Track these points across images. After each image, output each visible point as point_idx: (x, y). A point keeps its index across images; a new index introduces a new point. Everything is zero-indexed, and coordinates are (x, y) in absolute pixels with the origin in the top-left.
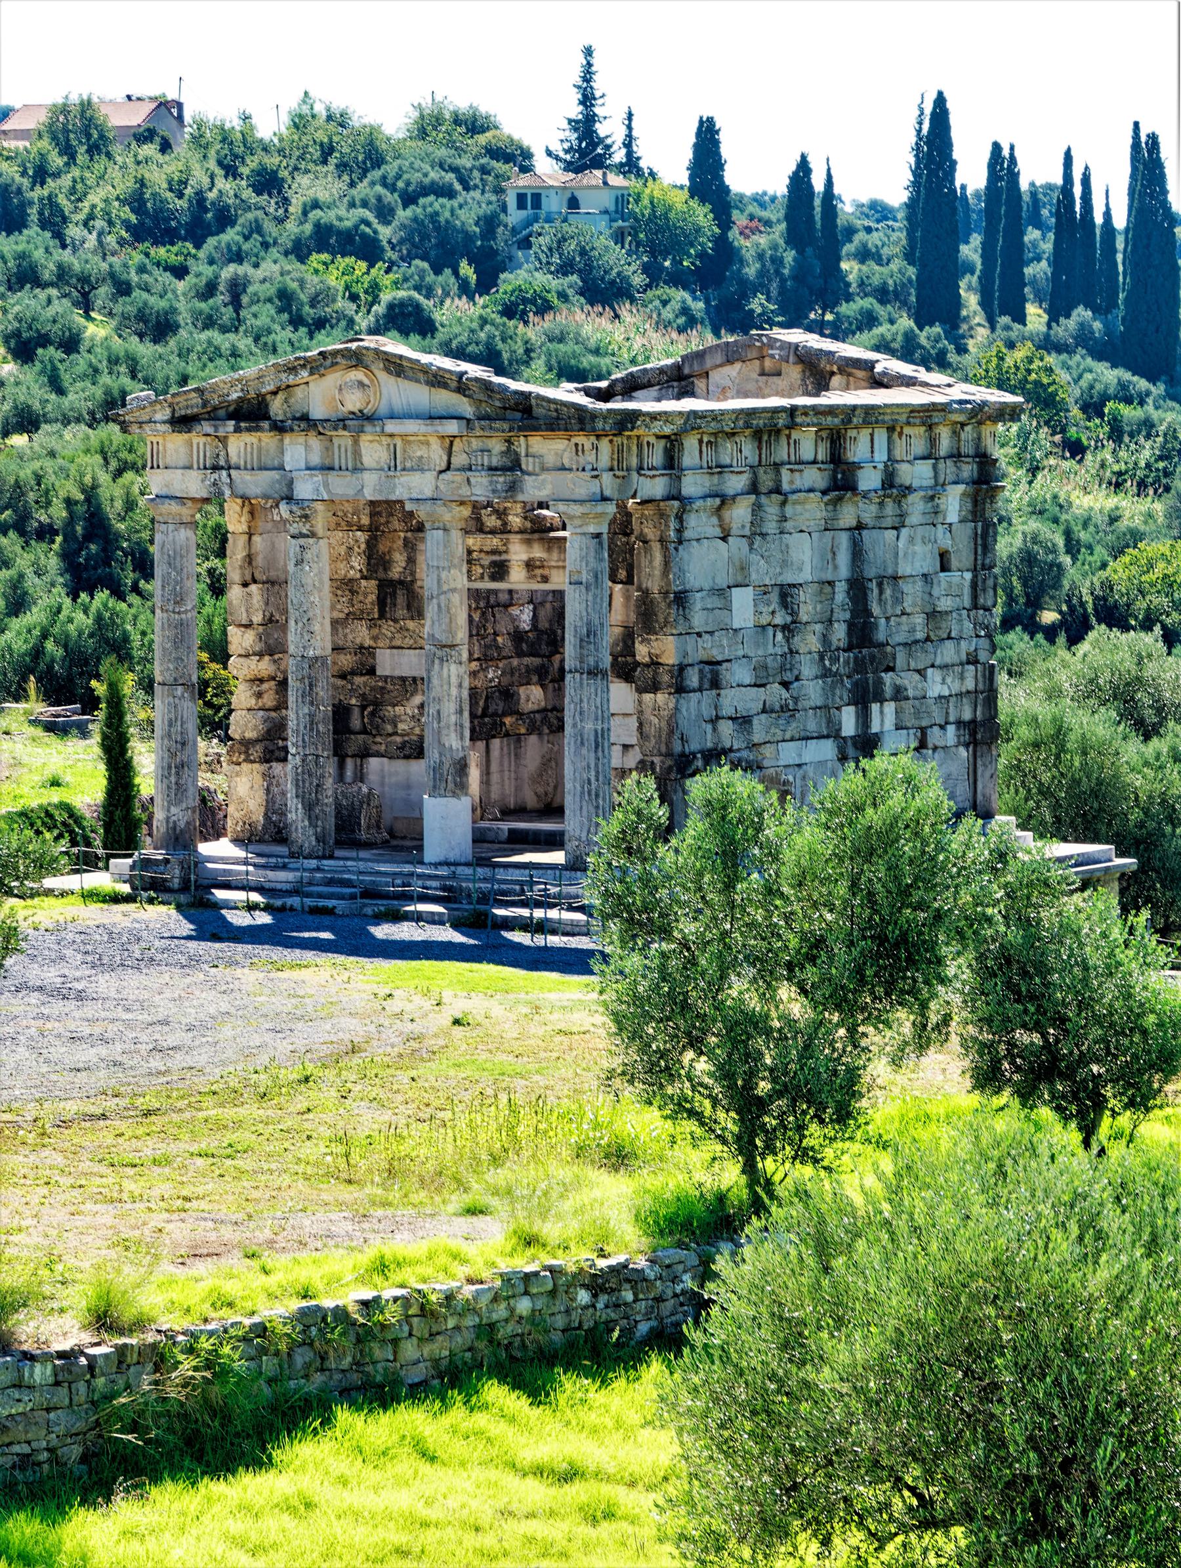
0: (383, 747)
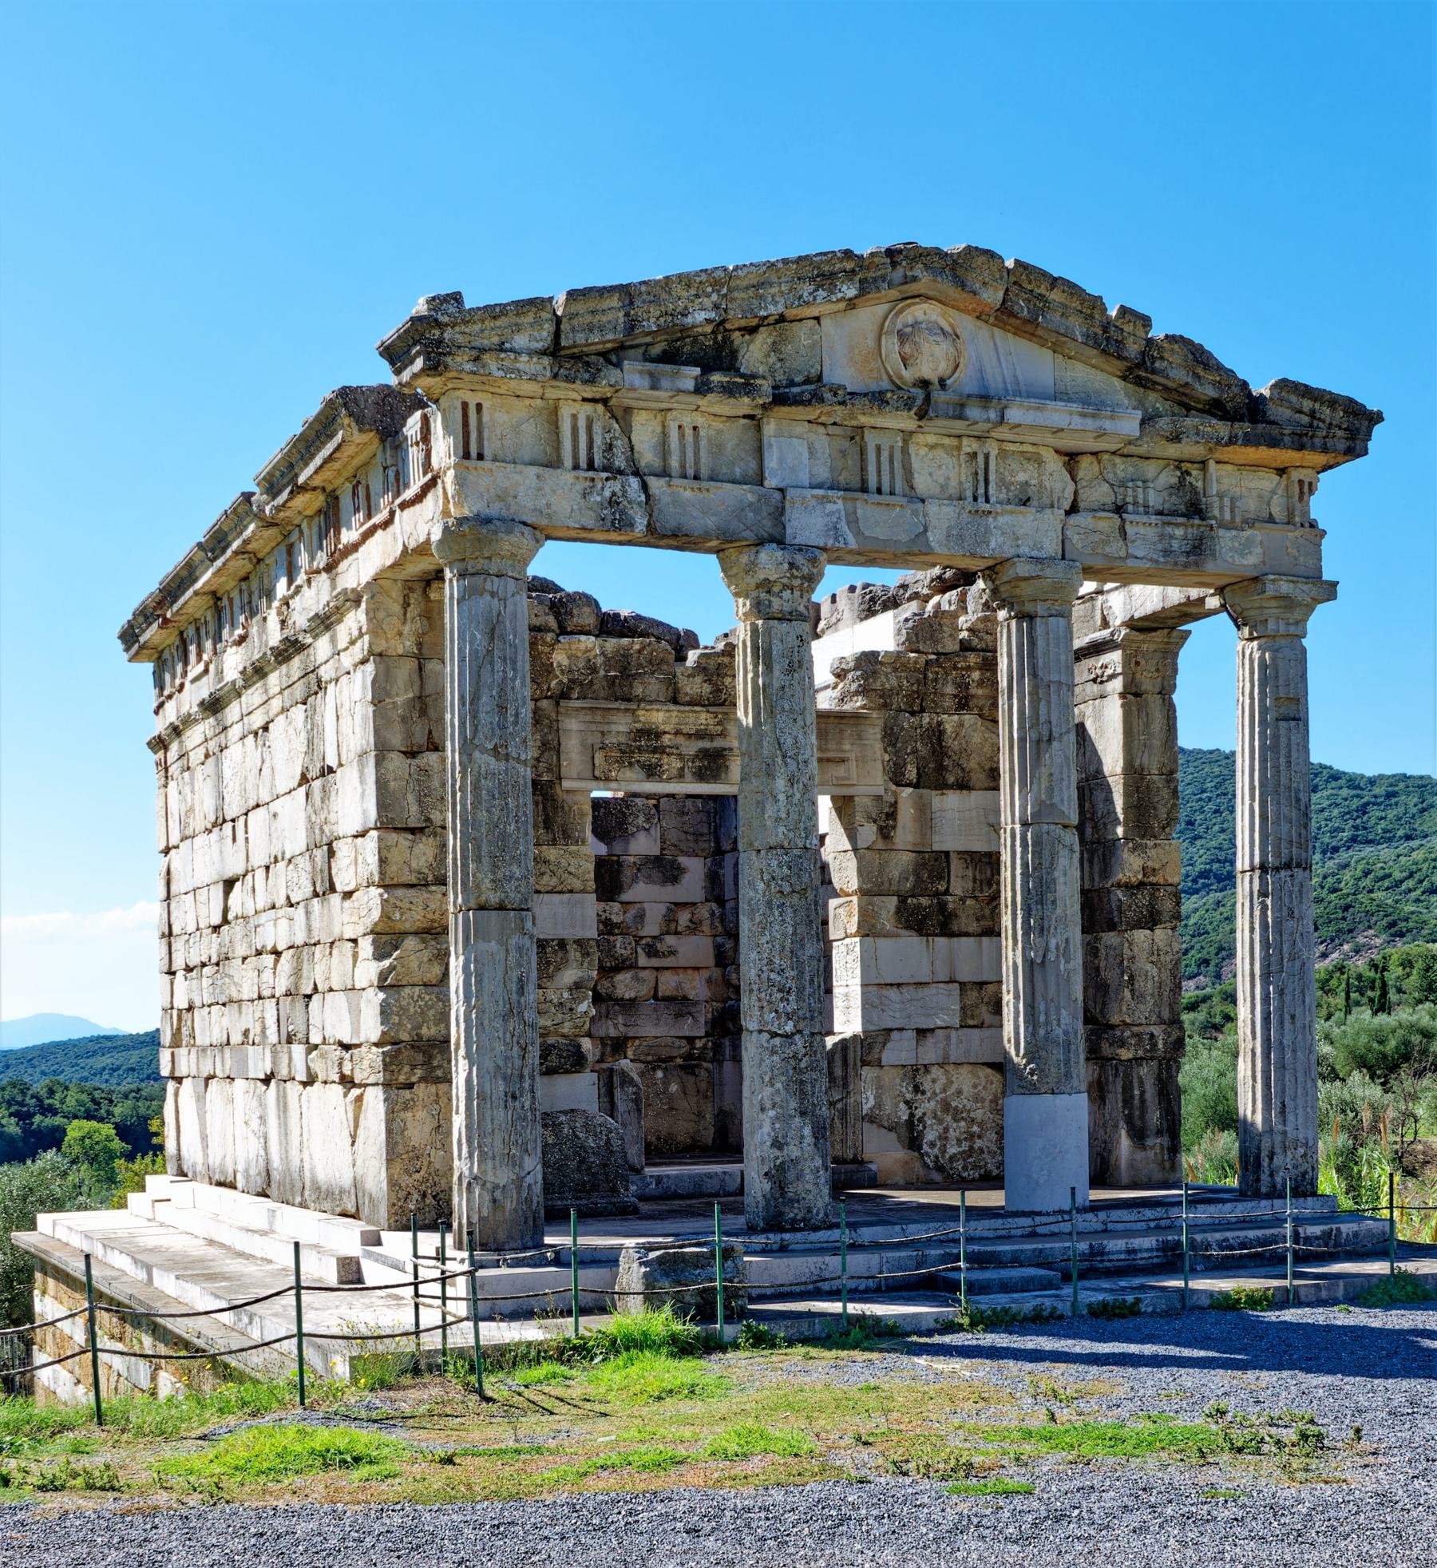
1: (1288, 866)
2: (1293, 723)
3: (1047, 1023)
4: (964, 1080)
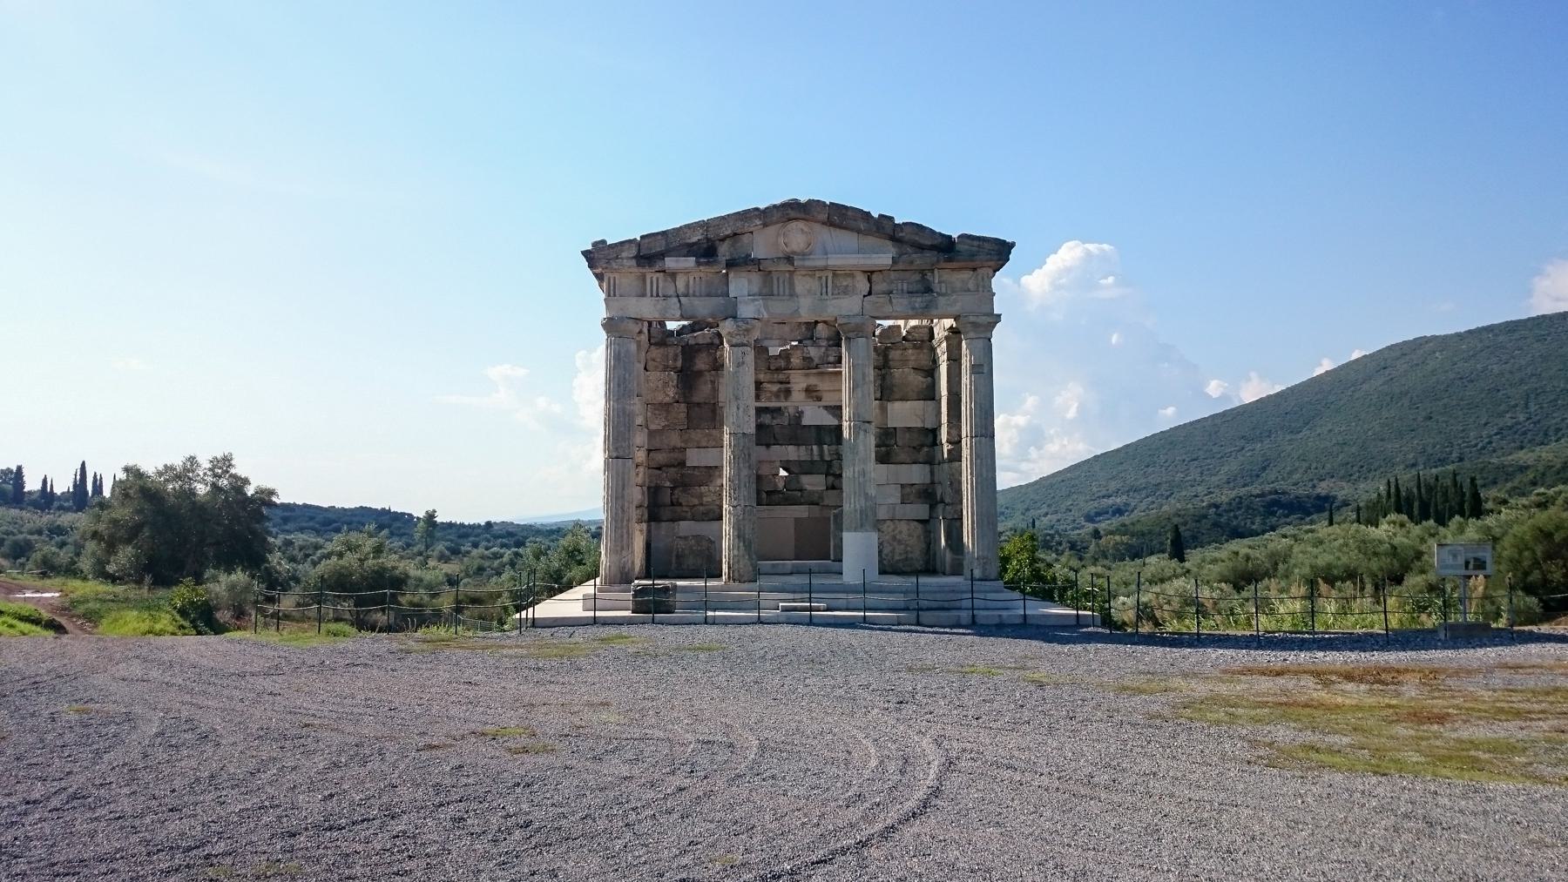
4: (903, 527)
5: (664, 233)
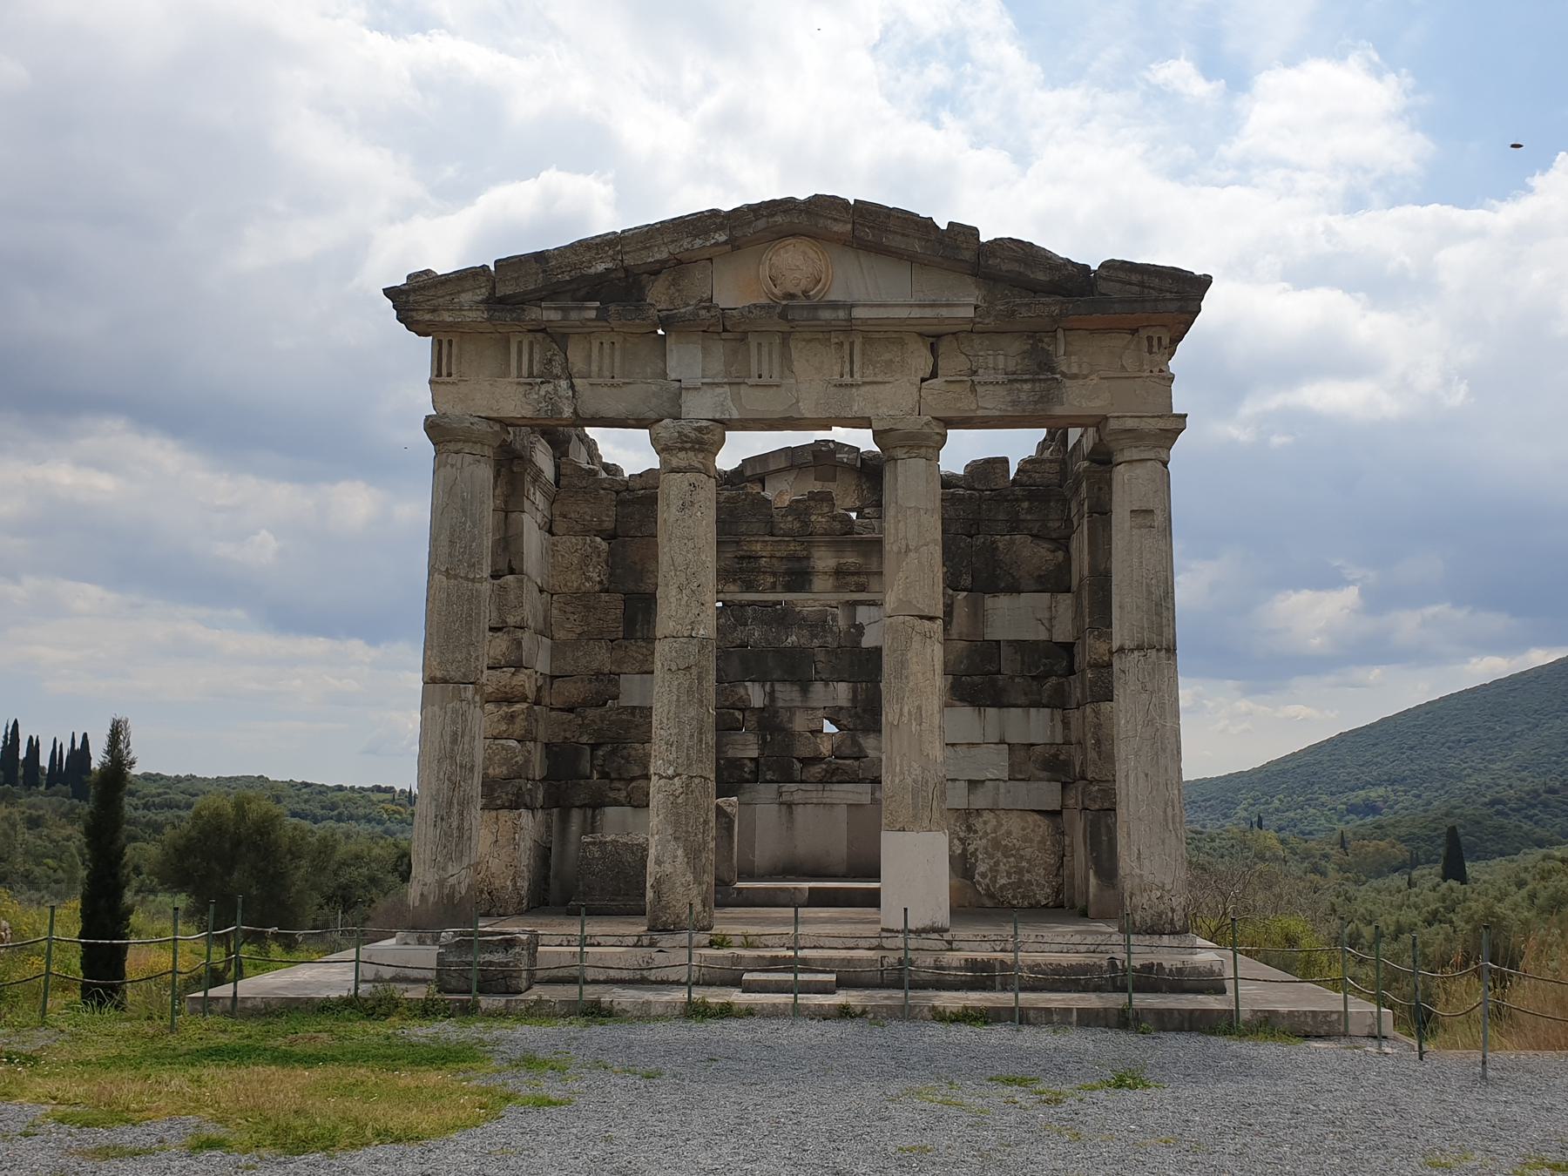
0: (624, 794)
1: (1140, 648)
2: (1144, 531)
3: (902, 773)
4: (1013, 824)
5: (540, 257)
